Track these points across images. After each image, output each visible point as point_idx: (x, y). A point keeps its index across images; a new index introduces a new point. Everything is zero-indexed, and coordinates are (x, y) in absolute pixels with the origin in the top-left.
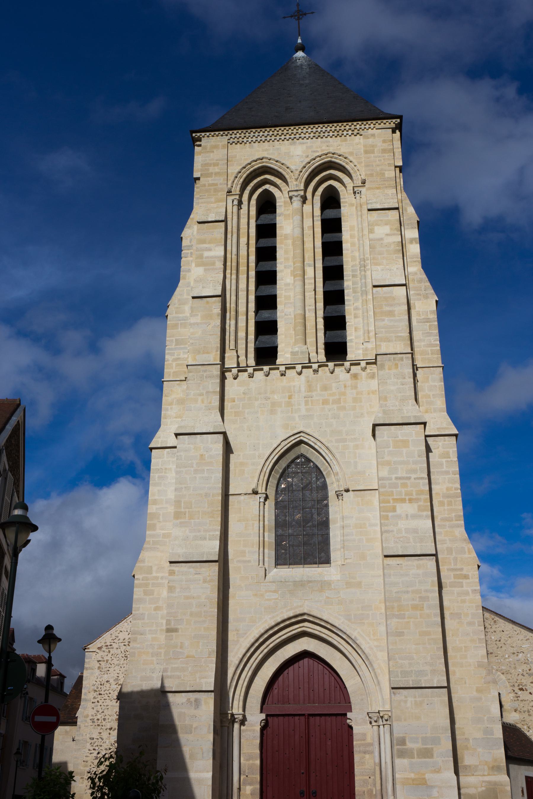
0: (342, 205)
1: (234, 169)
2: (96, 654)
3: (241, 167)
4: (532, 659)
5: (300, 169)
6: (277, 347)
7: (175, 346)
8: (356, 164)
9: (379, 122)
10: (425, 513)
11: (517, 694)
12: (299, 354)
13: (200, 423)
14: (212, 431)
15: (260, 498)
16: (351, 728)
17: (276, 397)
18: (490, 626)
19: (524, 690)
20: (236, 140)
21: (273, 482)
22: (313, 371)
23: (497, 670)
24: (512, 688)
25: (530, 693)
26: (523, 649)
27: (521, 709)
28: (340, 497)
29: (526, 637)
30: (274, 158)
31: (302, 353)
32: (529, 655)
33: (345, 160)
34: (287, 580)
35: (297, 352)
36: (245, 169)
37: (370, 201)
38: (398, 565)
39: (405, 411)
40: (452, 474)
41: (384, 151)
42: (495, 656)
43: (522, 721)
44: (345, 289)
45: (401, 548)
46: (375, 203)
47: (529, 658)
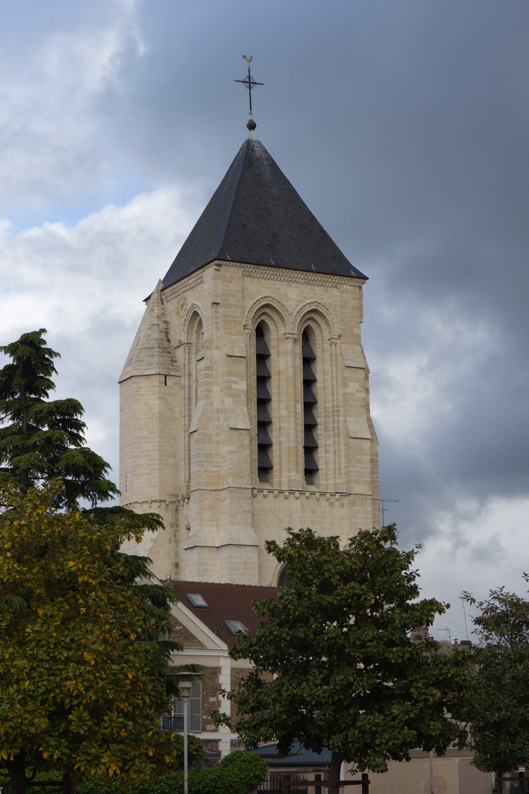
35: (295, 480)
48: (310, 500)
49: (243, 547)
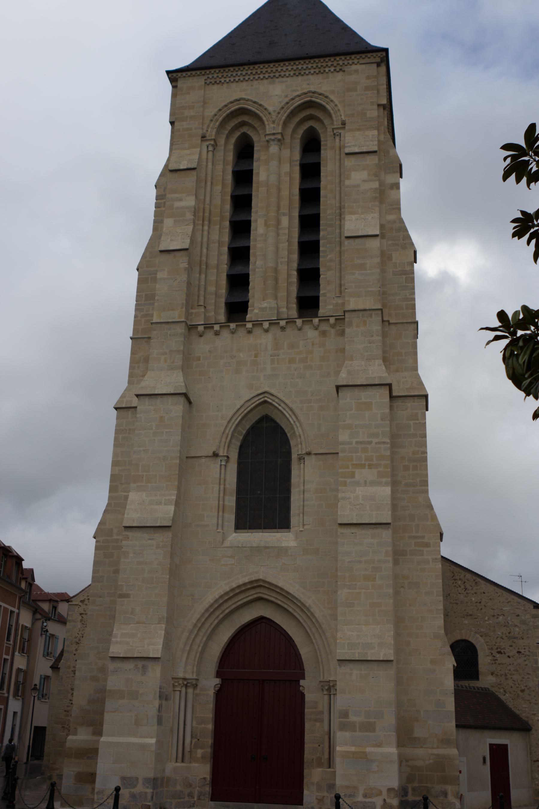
0: (322, 148)
1: (210, 111)
2: (79, 607)
3: (217, 110)
4: (512, 622)
5: (278, 110)
6: (248, 301)
7: (144, 301)
8: (337, 103)
9: (363, 56)
10: (384, 480)
11: (494, 657)
12: (268, 310)
13: (161, 384)
14: (172, 392)
15: (221, 460)
16: (303, 695)
17: (241, 355)
18: (471, 588)
19: (502, 654)
20: (213, 81)
21: (237, 444)
22: (281, 328)
23: (476, 632)
24: (490, 651)
25: (509, 657)
26: (504, 612)
27: (498, 673)
28: (302, 461)
29: (508, 599)
30: (252, 99)
31: (271, 308)
32: (509, 618)
33: (326, 99)
34: (244, 546)
35: (266, 308)
36: (221, 112)
37: (349, 144)
38: (353, 533)
39: (371, 372)
40: (420, 437)
41: (367, 88)
42: (475, 618)
43: (498, 684)
44: (320, 239)
45: (356, 516)
46: (354, 146)
47: (509, 620)
48: (288, 330)
49: (159, 397)
